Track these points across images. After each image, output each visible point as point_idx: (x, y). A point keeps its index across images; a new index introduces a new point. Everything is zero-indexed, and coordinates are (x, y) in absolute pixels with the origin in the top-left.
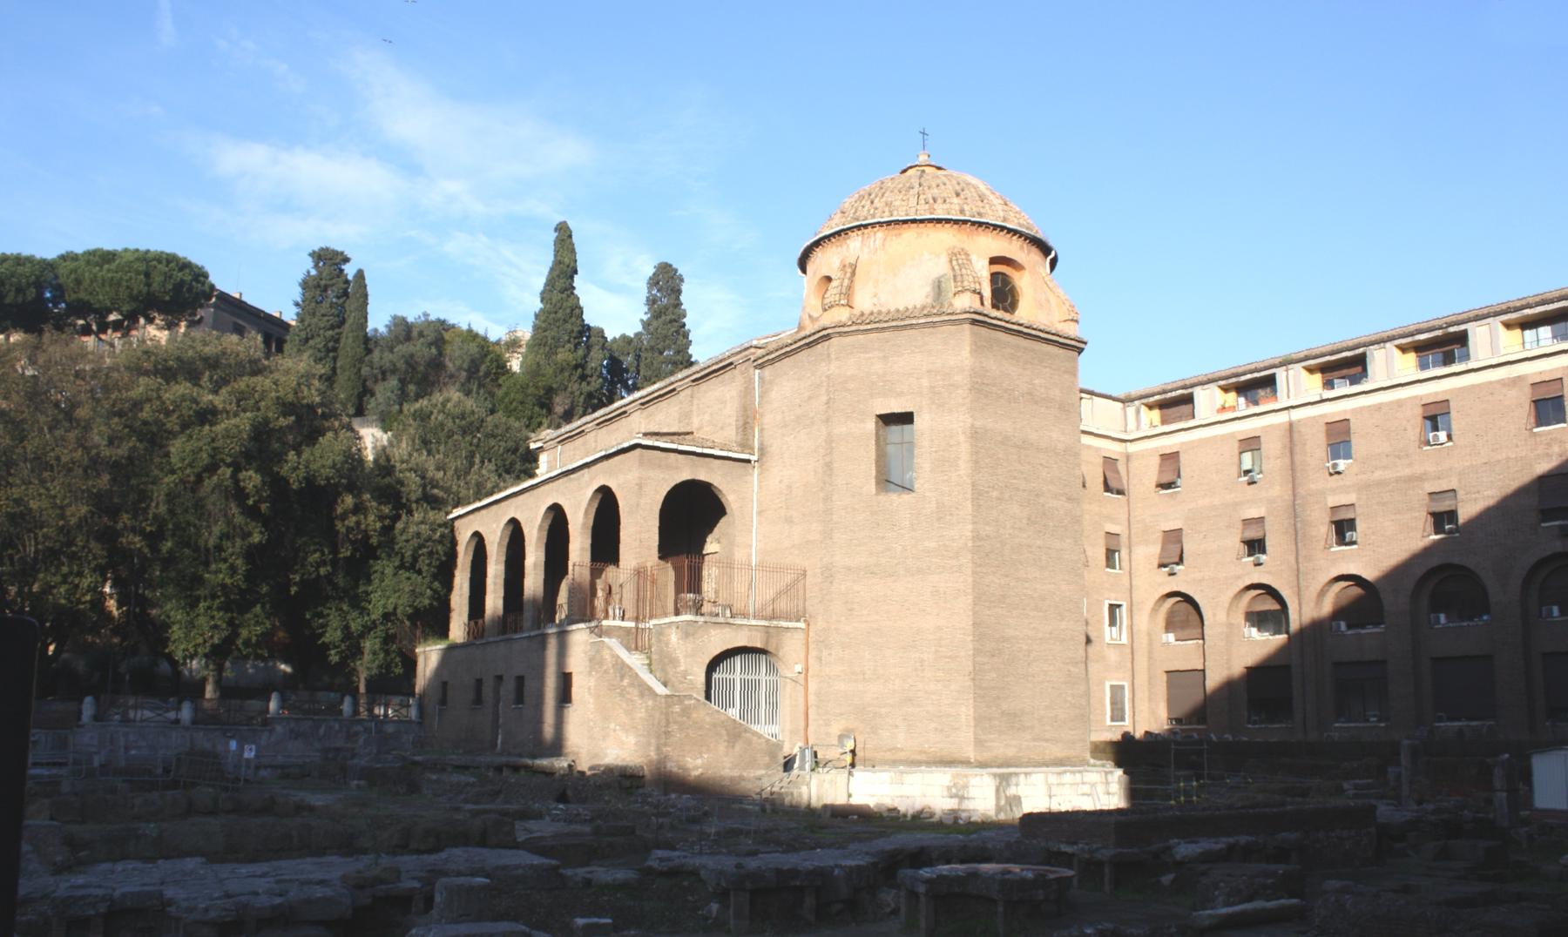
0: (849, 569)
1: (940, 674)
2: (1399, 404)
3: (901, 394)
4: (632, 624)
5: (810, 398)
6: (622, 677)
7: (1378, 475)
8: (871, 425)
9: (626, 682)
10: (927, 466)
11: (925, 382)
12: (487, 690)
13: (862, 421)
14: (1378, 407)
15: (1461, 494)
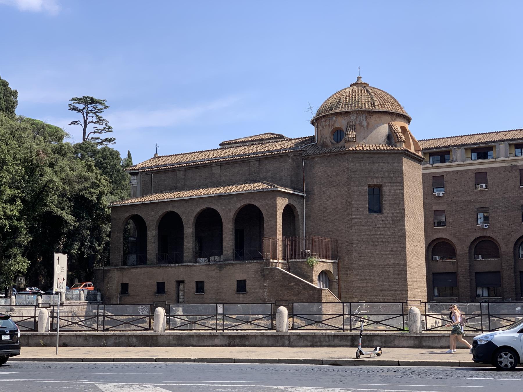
0: (359, 241)
1: (395, 280)
2: (466, 171)
3: (377, 178)
4: (280, 261)
5: (336, 175)
6: (290, 282)
7: (456, 199)
8: (366, 188)
9: (292, 284)
10: (388, 205)
11: (386, 174)
12: (171, 287)
13: (363, 186)
14: (457, 172)
15: (491, 208)
